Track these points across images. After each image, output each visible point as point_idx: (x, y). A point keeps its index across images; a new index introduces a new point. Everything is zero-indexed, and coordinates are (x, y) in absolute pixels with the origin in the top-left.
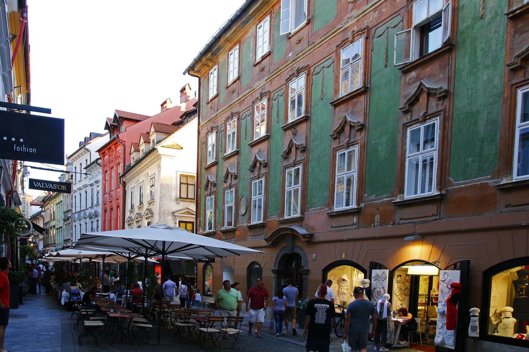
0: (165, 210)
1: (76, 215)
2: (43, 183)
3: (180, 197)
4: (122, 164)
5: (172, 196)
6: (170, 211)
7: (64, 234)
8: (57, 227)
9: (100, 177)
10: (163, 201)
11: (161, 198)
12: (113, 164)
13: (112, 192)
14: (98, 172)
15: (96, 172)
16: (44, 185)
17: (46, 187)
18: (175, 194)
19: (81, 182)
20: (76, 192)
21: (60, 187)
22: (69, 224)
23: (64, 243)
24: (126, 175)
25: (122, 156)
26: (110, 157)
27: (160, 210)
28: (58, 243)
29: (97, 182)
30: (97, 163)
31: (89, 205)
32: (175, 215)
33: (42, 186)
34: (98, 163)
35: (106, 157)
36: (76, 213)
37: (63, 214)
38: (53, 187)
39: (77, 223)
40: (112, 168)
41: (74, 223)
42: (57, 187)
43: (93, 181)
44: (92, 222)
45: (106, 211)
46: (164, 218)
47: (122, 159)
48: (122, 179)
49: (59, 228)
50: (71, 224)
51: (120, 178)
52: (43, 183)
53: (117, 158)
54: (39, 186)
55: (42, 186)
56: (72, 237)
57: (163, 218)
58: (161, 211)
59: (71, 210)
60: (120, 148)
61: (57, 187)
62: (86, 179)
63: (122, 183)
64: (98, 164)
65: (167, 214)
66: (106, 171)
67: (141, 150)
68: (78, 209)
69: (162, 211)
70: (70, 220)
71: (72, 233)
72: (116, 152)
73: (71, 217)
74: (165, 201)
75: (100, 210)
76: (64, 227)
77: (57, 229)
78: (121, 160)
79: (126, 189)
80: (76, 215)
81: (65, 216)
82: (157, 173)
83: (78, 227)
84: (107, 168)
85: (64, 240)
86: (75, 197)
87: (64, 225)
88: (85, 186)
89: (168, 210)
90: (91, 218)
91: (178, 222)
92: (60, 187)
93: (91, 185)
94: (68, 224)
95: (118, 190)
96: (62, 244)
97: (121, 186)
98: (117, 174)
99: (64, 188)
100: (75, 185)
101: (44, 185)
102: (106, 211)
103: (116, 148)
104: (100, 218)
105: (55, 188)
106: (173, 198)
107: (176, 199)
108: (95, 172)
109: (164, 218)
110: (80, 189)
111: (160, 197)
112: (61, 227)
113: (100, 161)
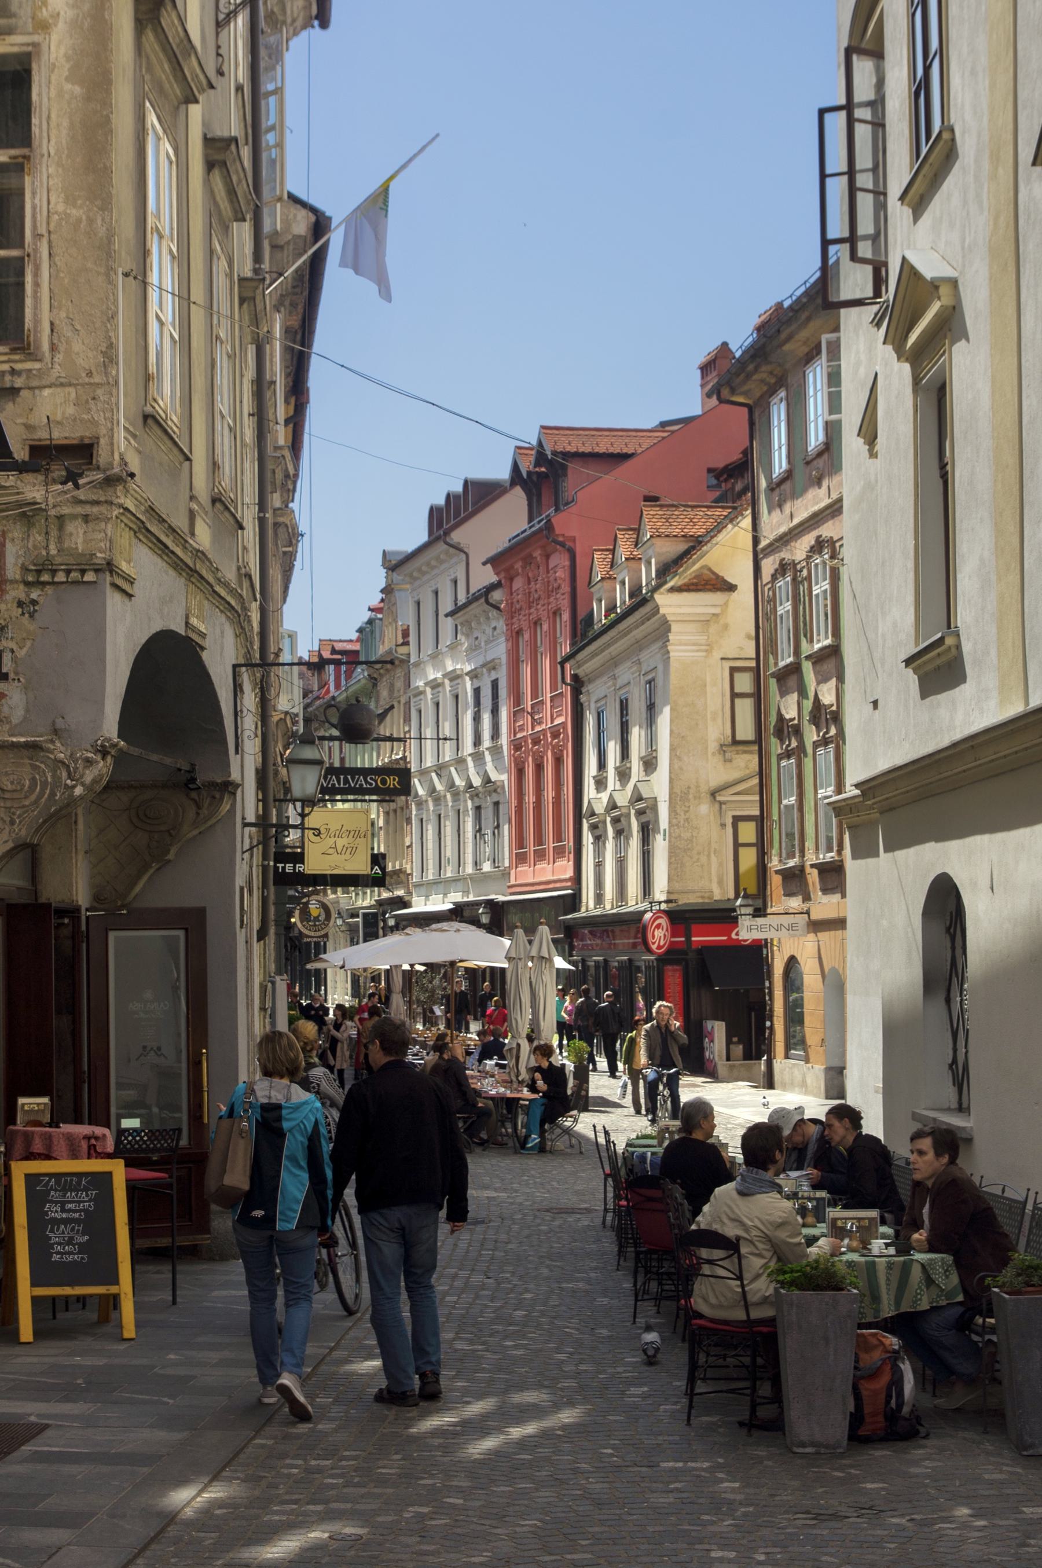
0: (689, 788)
3: (735, 742)
4: (566, 616)
5: (706, 741)
6: (704, 788)
9: (500, 650)
10: (679, 758)
11: (673, 749)
12: (541, 611)
14: (495, 628)
15: (489, 631)
16: (346, 781)
18: (716, 731)
22: (399, 811)
25: (566, 588)
26: (529, 583)
27: (671, 788)
30: (487, 602)
32: (719, 798)
33: (339, 783)
34: (491, 601)
35: (518, 583)
38: (367, 782)
40: (537, 623)
42: (376, 782)
46: (686, 812)
47: (567, 597)
48: (568, 666)
51: (562, 664)
53: (551, 590)
54: (333, 785)
55: (339, 783)
57: (682, 814)
58: (675, 790)
60: (559, 561)
61: (376, 782)
65: (695, 798)
66: (519, 633)
69: (677, 790)
72: (548, 572)
74: (685, 759)
78: (565, 603)
79: (583, 698)
82: (660, 668)
89: (698, 787)
91: (729, 821)
92: (384, 782)
94: (395, 811)
97: (568, 691)
99: (392, 782)
101: (346, 781)
105: (371, 784)
106: (713, 746)
107: (722, 748)
108: (484, 627)
111: (671, 745)
113: (497, 596)
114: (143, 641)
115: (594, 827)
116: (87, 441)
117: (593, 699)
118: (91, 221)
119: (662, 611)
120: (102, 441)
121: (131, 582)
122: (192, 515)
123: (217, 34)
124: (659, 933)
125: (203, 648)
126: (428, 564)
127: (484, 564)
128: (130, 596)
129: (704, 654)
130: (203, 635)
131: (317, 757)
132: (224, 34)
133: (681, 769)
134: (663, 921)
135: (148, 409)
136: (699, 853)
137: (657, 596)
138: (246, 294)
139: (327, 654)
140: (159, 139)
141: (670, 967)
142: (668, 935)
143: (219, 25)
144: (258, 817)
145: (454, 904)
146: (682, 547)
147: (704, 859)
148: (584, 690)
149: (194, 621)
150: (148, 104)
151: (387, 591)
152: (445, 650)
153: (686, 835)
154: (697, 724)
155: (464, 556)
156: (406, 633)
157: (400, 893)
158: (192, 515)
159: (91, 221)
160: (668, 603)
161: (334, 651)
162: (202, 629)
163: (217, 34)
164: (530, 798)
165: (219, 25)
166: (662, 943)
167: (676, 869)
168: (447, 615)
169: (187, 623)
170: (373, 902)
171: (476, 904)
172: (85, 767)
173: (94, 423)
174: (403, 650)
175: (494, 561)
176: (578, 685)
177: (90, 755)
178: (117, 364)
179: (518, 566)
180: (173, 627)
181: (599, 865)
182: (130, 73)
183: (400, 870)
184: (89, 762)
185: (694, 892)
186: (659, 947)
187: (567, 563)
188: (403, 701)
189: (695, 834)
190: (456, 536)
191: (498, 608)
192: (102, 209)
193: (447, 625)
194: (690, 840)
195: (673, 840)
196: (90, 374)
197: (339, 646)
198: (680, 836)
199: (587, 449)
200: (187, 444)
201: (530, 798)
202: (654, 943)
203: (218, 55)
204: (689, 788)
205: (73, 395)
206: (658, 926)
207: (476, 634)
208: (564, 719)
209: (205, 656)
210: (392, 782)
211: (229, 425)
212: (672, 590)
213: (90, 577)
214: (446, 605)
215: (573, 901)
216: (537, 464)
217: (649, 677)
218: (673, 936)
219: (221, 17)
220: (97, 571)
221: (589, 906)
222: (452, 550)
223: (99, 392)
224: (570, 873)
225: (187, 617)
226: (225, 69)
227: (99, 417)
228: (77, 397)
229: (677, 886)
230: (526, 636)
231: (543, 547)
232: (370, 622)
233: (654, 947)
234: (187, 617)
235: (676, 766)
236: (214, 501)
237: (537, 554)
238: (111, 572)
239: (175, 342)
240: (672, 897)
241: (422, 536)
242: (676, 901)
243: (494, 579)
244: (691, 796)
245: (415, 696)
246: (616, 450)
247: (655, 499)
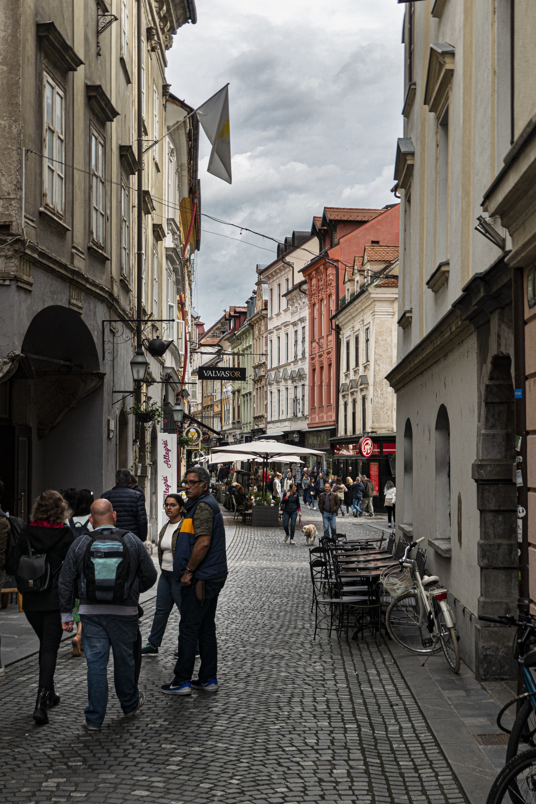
1: (273, 373)
4: (334, 297)
7: (255, 406)
8: (243, 392)
9: (306, 313)
10: (379, 365)
11: (376, 361)
13: (322, 341)
15: (301, 304)
16: (216, 373)
19: (279, 317)
20: (272, 332)
21: (233, 374)
23: (254, 422)
24: (339, 317)
25: (334, 284)
28: (246, 422)
29: (302, 320)
30: (300, 290)
31: (291, 359)
35: (314, 282)
36: (272, 369)
37: (252, 369)
39: (274, 388)
40: (322, 300)
41: (269, 388)
43: (296, 318)
44: (296, 387)
45: (314, 370)
47: (334, 288)
48: (333, 321)
49: (246, 394)
50: (265, 388)
53: (327, 285)
56: (266, 412)
59: (264, 363)
62: (288, 313)
63: (334, 327)
66: (314, 305)
67: (356, 280)
68: (275, 365)
69: (377, 380)
70: (263, 382)
71: (266, 405)
73: (264, 376)
74: (382, 365)
75: (306, 366)
76: (254, 393)
77: (243, 396)
78: (334, 291)
79: (341, 336)
80: (273, 373)
81: (256, 375)
83: (275, 394)
84: (315, 300)
85: (255, 418)
86: (271, 341)
87: (254, 388)
88: (286, 324)
90: (293, 379)
92: (233, 374)
93: (294, 324)
95: (330, 338)
96: (252, 424)
98: (329, 310)
99: (237, 374)
100: (271, 321)
101: (216, 373)
102: (314, 370)
103: (327, 269)
104: (307, 382)
108: (299, 302)
110: (278, 329)
112: (250, 393)
113: (305, 287)
114: (39, 310)
115: (344, 396)
116: (7, 223)
117: (345, 337)
118: (10, 127)
120: (14, 224)
121: (31, 285)
122: (72, 255)
123: (98, 37)
124: (368, 447)
125: (81, 314)
126: (275, 271)
127: (299, 272)
128: (30, 291)
130: (81, 308)
131: (144, 361)
132: (101, 36)
134: (369, 442)
135: (42, 209)
137: (369, 289)
138: (123, 153)
139: (232, 313)
140: (53, 88)
141: (372, 463)
143: (98, 33)
144: (134, 389)
145: (284, 432)
146: (383, 266)
147: (389, 413)
148: (341, 332)
149: (74, 301)
150: (45, 73)
151: (259, 284)
152: (282, 312)
155: (291, 268)
156: (266, 303)
157: (262, 426)
158: (72, 255)
159: (10, 127)
160: (374, 293)
161: (235, 312)
162: (80, 304)
163: (98, 37)
164: (317, 383)
165: (98, 33)
168: (283, 296)
169: (70, 303)
170: (249, 430)
171: (293, 432)
172: (3, 365)
173: (10, 215)
174: (264, 312)
175: (303, 271)
176: (338, 329)
177: (6, 360)
178: (22, 190)
179: (314, 273)
180: (60, 304)
181: (346, 416)
182: (32, 60)
183: (262, 416)
184: (5, 363)
185: (384, 428)
186: (367, 454)
187: (335, 272)
188: (264, 336)
190: (288, 259)
191: (305, 293)
192: (15, 121)
193: (284, 300)
196: (9, 194)
197: (238, 310)
199: (345, 218)
200: (71, 225)
201: (317, 383)
203: (98, 46)
205: (2, 203)
206: (367, 444)
207: (296, 305)
208: (333, 344)
209: (82, 317)
210: (237, 374)
211: (101, 213)
212: (377, 286)
213: (7, 283)
214: (284, 291)
215: (334, 432)
216: (323, 225)
217: (367, 327)
219: (100, 29)
220: (10, 280)
221: (341, 433)
222: (286, 265)
223: (13, 202)
224: (334, 418)
225: (70, 300)
226: (101, 52)
227: (13, 213)
228: (3, 204)
229: (376, 425)
230: (317, 307)
231: (324, 264)
232: (251, 298)
233: (365, 454)
234: (70, 300)
235: (377, 369)
236: (89, 248)
237: (322, 267)
238: (17, 281)
239: (62, 178)
240: (374, 430)
241: (274, 257)
242: (376, 432)
243: (303, 279)
245: (270, 333)
246: (359, 219)
247: (378, 242)
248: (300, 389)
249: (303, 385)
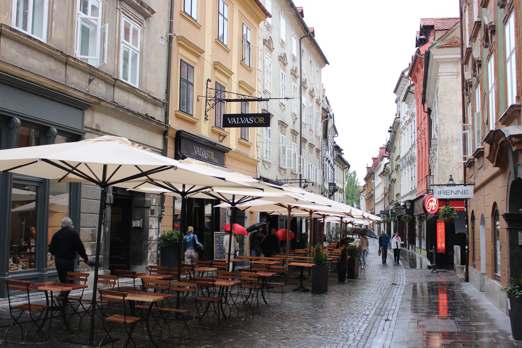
2: (238, 118)
10: (444, 124)
16: (240, 120)
17: (241, 122)
21: (257, 120)
33: (236, 122)
38: (249, 121)
46: (446, 149)
52: (238, 118)
55: (236, 122)
57: (445, 150)
61: (253, 120)
63: (426, 110)
64: (411, 92)
65: (451, 142)
89: (452, 137)
92: (257, 120)
99: (261, 120)
101: (240, 120)
105: (251, 122)
109: (446, 149)
113: (413, 89)
119: (435, 57)
129: (456, 77)
133: (444, 129)
136: (453, 168)
137: (431, 50)
142: (437, 205)
153: (447, 159)
154: (452, 109)
166: (434, 209)
167: (442, 175)
186: (432, 210)
189: (451, 159)
194: (449, 162)
195: (440, 162)
198: (444, 160)
202: (429, 209)
204: (448, 138)
206: (431, 201)
210: (261, 120)
218: (439, 206)
244: (449, 142)
248: (413, 169)
249: (415, 165)
